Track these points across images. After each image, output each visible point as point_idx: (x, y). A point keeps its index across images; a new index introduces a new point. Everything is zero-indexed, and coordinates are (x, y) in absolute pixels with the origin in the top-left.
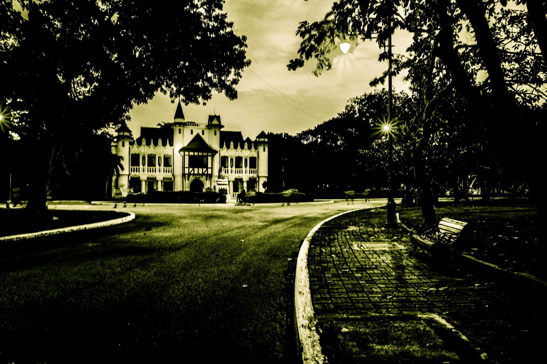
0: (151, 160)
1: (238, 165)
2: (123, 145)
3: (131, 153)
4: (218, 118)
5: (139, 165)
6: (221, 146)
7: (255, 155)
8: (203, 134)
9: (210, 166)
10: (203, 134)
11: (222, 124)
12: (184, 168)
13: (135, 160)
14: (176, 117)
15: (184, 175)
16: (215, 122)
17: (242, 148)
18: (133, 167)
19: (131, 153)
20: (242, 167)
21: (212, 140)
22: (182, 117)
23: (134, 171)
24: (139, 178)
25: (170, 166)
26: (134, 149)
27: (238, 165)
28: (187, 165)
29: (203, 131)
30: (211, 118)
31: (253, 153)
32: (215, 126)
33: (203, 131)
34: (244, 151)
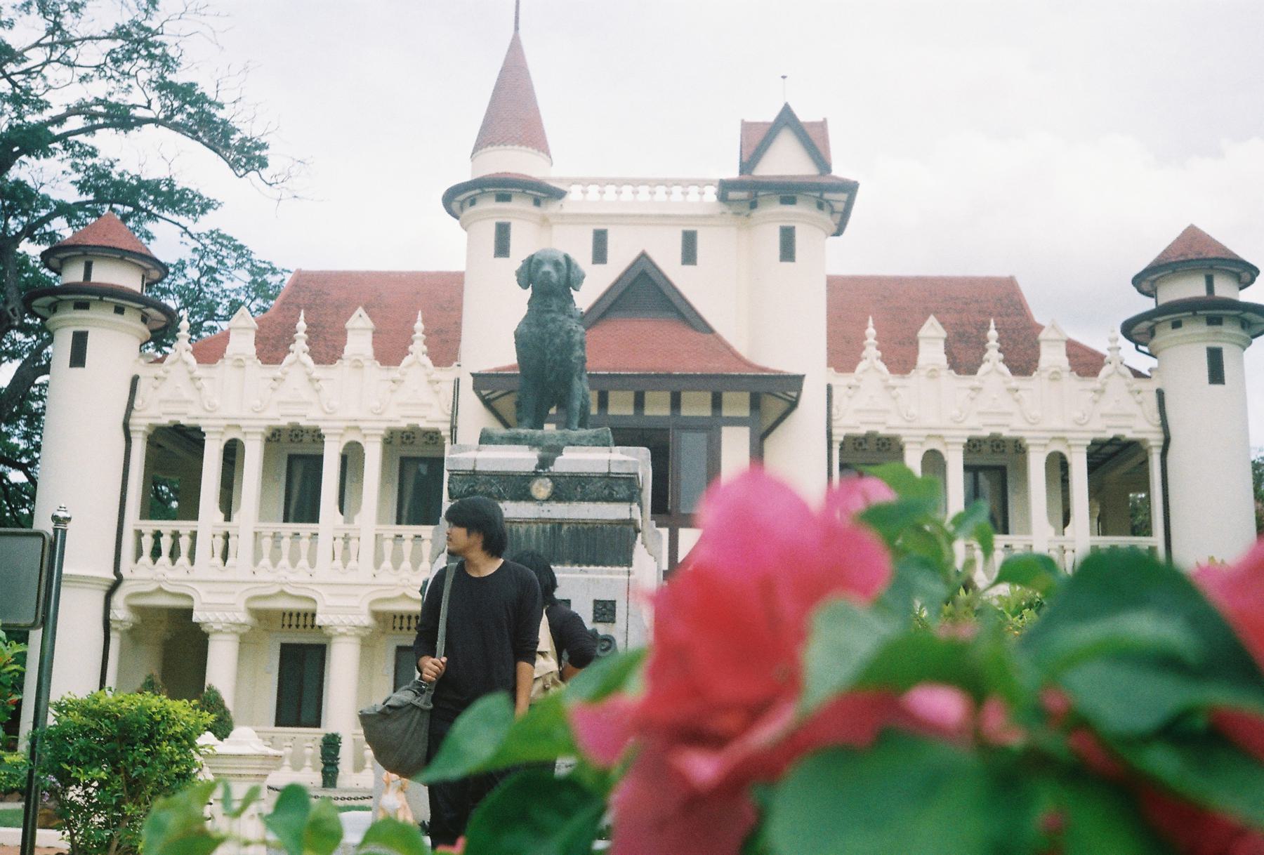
0: (299, 471)
2: (78, 358)
3: (141, 424)
4: (813, 141)
5: (190, 510)
6: (843, 354)
8: (689, 255)
10: (689, 255)
11: (840, 170)
13: (172, 465)
14: (488, 137)
16: (785, 161)
17: (1022, 360)
18: (150, 526)
19: (141, 424)
20: (1026, 529)
21: (761, 307)
22: (533, 137)
24: (189, 612)
29: (689, 241)
30: (758, 142)
31: (1121, 413)
32: (788, 192)
33: (689, 241)
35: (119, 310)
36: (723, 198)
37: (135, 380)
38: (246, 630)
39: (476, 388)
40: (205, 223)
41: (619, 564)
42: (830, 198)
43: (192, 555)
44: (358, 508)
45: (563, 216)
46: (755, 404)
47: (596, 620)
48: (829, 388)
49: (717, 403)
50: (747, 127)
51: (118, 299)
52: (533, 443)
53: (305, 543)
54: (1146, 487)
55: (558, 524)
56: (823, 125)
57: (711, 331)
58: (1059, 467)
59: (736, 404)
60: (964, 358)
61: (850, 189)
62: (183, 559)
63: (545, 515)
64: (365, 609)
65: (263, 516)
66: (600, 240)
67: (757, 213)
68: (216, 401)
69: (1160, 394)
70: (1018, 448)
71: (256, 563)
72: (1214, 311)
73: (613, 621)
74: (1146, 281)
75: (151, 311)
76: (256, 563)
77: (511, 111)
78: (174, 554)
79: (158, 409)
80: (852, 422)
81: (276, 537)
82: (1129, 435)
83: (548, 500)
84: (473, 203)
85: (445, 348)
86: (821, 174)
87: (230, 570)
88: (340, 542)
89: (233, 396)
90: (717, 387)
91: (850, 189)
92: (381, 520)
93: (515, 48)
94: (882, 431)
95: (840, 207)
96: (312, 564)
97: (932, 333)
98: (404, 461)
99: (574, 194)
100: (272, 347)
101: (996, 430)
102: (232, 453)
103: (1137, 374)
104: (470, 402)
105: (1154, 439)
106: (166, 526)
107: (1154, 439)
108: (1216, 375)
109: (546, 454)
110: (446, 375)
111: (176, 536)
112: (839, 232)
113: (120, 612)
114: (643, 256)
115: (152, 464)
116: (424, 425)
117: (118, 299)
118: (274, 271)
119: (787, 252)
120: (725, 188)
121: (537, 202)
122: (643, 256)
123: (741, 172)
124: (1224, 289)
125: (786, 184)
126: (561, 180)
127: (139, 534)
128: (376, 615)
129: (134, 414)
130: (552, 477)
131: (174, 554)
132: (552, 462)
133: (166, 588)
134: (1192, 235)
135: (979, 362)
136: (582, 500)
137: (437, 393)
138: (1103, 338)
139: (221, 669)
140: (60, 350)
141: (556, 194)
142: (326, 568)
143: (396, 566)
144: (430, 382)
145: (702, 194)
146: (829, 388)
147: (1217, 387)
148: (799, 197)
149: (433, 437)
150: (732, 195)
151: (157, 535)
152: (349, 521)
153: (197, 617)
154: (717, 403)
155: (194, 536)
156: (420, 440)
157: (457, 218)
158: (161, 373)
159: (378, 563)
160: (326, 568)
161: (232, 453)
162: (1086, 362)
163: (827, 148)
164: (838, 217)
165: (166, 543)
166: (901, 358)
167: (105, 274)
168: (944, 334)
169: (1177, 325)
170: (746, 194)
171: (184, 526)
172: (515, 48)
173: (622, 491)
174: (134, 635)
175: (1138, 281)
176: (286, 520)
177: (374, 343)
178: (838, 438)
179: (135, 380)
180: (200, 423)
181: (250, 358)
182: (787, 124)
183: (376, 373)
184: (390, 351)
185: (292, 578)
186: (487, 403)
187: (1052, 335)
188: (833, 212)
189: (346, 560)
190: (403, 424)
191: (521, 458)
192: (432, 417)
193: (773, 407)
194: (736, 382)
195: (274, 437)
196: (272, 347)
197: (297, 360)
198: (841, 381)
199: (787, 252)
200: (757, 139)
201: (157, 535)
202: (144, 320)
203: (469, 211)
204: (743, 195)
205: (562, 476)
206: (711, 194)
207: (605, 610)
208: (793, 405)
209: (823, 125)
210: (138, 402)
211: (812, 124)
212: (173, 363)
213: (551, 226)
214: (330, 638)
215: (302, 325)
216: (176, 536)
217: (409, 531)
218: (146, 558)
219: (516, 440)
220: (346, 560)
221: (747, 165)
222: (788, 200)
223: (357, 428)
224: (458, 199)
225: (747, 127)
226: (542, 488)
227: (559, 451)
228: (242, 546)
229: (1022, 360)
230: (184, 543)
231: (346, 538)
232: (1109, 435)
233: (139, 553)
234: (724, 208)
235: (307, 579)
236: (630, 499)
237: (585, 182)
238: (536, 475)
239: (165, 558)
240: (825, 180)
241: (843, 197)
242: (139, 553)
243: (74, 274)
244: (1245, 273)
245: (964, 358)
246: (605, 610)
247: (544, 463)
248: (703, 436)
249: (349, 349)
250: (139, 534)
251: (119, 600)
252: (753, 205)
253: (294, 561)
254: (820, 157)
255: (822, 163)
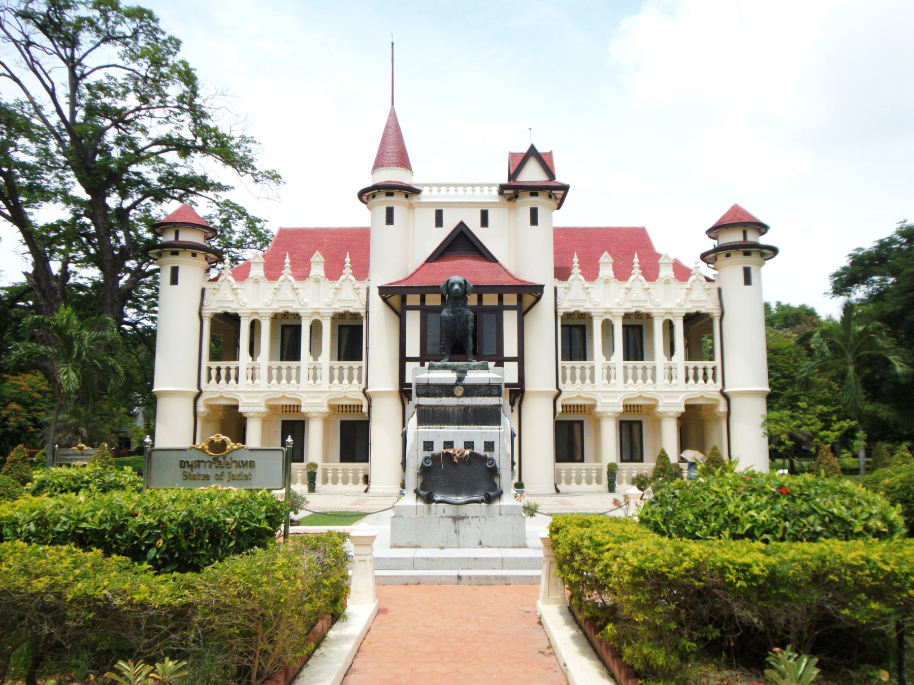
0: (289, 337)
1: (635, 347)
2: (174, 281)
5: (235, 357)
6: (562, 273)
7: (708, 306)
8: (484, 222)
9: (510, 348)
10: (484, 222)
11: (561, 178)
12: (403, 359)
13: (224, 335)
15: (405, 392)
16: (532, 174)
17: (651, 272)
18: (215, 365)
20: (652, 358)
21: (520, 248)
22: (404, 162)
23: (218, 379)
24: (237, 407)
25: (361, 360)
26: (219, 296)
27: (635, 347)
28: (413, 349)
29: (484, 216)
30: (518, 163)
32: (534, 190)
33: (484, 216)
34: (657, 287)
35: (194, 255)
36: (501, 193)
37: (203, 290)
38: (265, 415)
39: (380, 294)
40: (223, 196)
41: (494, 424)
42: (556, 192)
43: (237, 379)
44: (319, 354)
45: (420, 203)
46: (520, 299)
47: (485, 450)
48: (556, 289)
49: (501, 299)
50: (513, 156)
51: (194, 249)
52: (454, 369)
53: (294, 372)
54: (712, 338)
55: (467, 407)
56: (550, 153)
57: (496, 261)
58: (669, 326)
59: (510, 299)
60: (622, 273)
61: (565, 188)
62: (233, 381)
63: (461, 403)
64: (326, 404)
65: (272, 358)
66: (439, 216)
67: (518, 201)
68: (245, 300)
69: (720, 290)
70: (649, 317)
71: (269, 382)
72: (747, 249)
73: (493, 450)
74: (714, 232)
75: (210, 255)
76: (269, 382)
77: (393, 150)
78: (228, 378)
79: (215, 306)
80: (566, 306)
81: (279, 369)
82: (703, 311)
83: (462, 396)
84: (374, 197)
85: (362, 271)
86: (550, 180)
87: (256, 385)
88: (312, 371)
89: (254, 298)
90: (500, 290)
91: (565, 188)
92: (331, 359)
93: (393, 115)
94: (582, 310)
95: (560, 197)
96: (298, 382)
97: (606, 260)
98: (341, 327)
99: (425, 191)
100: (272, 271)
101: (638, 309)
102: (255, 326)
103: (708, 280)
104: (376, 301)
105: (716, 313)
106: (223, 364)
107: (716, 313)
108: (748, 281)
109: (460, 375)
110: (363, 285)
111: (228, 369)
112: (558, 208)
113: (201, 408)
114: (462, 224)
115: (213, 330)
116: (352, 311)
117: (194, 249)
118: (259, 221)
119: (534, 221)
120: (502, 188)
121: (407, 196)
122: (462, 223)
123: (510, 179)
124: (752, 237)
125: (532, 184)
126: (418, 185)
127: (210, 369)
128: (331, 407)
129: (204, 308)
130: (464, 386)
131: (228, 378)
132: (463, 379)
133: (224, 395)
134: (736, 209)
135: (630, 274)
136: (478, 396)
137: (358, 294)
138: (691, 260)
139: (254, 436)
140: (165, 276)
141: (417, 192)
142: (306, 383)
143: (341, 382)
144: (355, 289)
145: (490, 191)
146: (556, 289)
147: (748, 287)
148: (540, 193)
149: (356, 316)
150: (506, 192)
151: (219, 369)
152: (316, 359)
153: (241, 410)
154: (501, 299)
155: (237, 369)
156: (348, 317)
157: (366, 203)
158: (216, 286)
159: (331, 380)
160: (306, 383)
161: (255, 326)
162: (682, 273)
163: (553, 166)
164: (558, 201)
165: (223, 373)
166: (591, 273)
167: (186, 236)
168: (612, 261)
169: (728, 255)
170: (512, 191)
171: (232, 364)
172: (393, 115)
173: (495, 392)
174: (207, 420)
175: (709, 232)
176: (282, 360)
177: (325, 270)
178: (560, 313)
179: (203, 290)
180: (238, 312)
181: (261, 278)
182: (533, 154)
183: (326, 284)
184: (333, 273)
185: (288, 389)
186: (385, 300)
187: (666, 261)
188: (556, 199)
189: (315, 379)
190: (342, 311)
191: (448, 377)
192: (357, 307)
193: (528, 299)
194: (510, 289)
195: (275, 317)
196: (272, 271)
197: (286, 279)
198: (561, 285)
199: (534, 221)
200: (517, 163)
201: (219, 369)
202: (206, 259)
203: (372, 201)
204: (511, 192)
205: (468, 385)
206: (495, 191)
207: (489, 446)
208: (538, 299)
209: (550, 153)
210: (205, 302)
211: (545, 154)
212: (222, 281)
213: (414, 208)
214: (308, 418)
215: (287, 260)
216: (228, 369)
217: (346, 364)
218: (213, 381)
219: (445, 368)
220: (315, 379)
221: (512, 176)
222: (534, 194)
223: (319, 313)
224: (366, 195)
225: (513, 156)
226: (459, 391)
227: (465, 372)
228: (263, 373)
229: (651, 272)
230: (233, 373)
231: (315, 369)
232: (694, 311)
233: (209, 378)
234: (502, 197)
235: (294, 389)
236: (499, 395)
237: (431, 185)
238: (456, 385)
239: (223, 381)
240: (552, 184)
241: (562, 192)
242: (209, 378)
243: (169, 237)
244: (762, 228)
245: (622, 273)
246: (489, 446)
247: (460, 379)
248: (493, 316)
249: (312, 273)
250: (210, 369)
251: (201, 402)
252: (517, 197)
253: (289, 379)
254: (549, 171)
255: (550, 174)
